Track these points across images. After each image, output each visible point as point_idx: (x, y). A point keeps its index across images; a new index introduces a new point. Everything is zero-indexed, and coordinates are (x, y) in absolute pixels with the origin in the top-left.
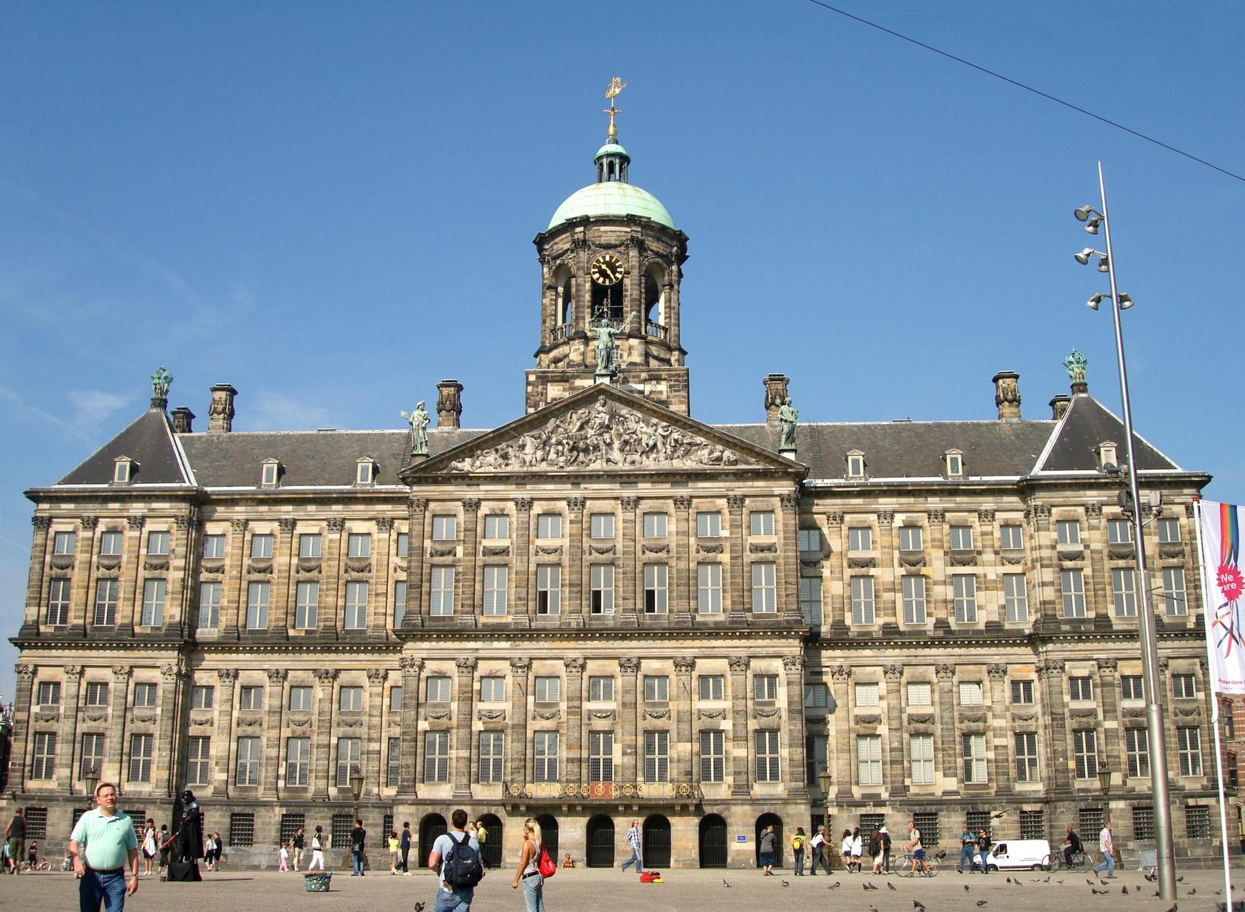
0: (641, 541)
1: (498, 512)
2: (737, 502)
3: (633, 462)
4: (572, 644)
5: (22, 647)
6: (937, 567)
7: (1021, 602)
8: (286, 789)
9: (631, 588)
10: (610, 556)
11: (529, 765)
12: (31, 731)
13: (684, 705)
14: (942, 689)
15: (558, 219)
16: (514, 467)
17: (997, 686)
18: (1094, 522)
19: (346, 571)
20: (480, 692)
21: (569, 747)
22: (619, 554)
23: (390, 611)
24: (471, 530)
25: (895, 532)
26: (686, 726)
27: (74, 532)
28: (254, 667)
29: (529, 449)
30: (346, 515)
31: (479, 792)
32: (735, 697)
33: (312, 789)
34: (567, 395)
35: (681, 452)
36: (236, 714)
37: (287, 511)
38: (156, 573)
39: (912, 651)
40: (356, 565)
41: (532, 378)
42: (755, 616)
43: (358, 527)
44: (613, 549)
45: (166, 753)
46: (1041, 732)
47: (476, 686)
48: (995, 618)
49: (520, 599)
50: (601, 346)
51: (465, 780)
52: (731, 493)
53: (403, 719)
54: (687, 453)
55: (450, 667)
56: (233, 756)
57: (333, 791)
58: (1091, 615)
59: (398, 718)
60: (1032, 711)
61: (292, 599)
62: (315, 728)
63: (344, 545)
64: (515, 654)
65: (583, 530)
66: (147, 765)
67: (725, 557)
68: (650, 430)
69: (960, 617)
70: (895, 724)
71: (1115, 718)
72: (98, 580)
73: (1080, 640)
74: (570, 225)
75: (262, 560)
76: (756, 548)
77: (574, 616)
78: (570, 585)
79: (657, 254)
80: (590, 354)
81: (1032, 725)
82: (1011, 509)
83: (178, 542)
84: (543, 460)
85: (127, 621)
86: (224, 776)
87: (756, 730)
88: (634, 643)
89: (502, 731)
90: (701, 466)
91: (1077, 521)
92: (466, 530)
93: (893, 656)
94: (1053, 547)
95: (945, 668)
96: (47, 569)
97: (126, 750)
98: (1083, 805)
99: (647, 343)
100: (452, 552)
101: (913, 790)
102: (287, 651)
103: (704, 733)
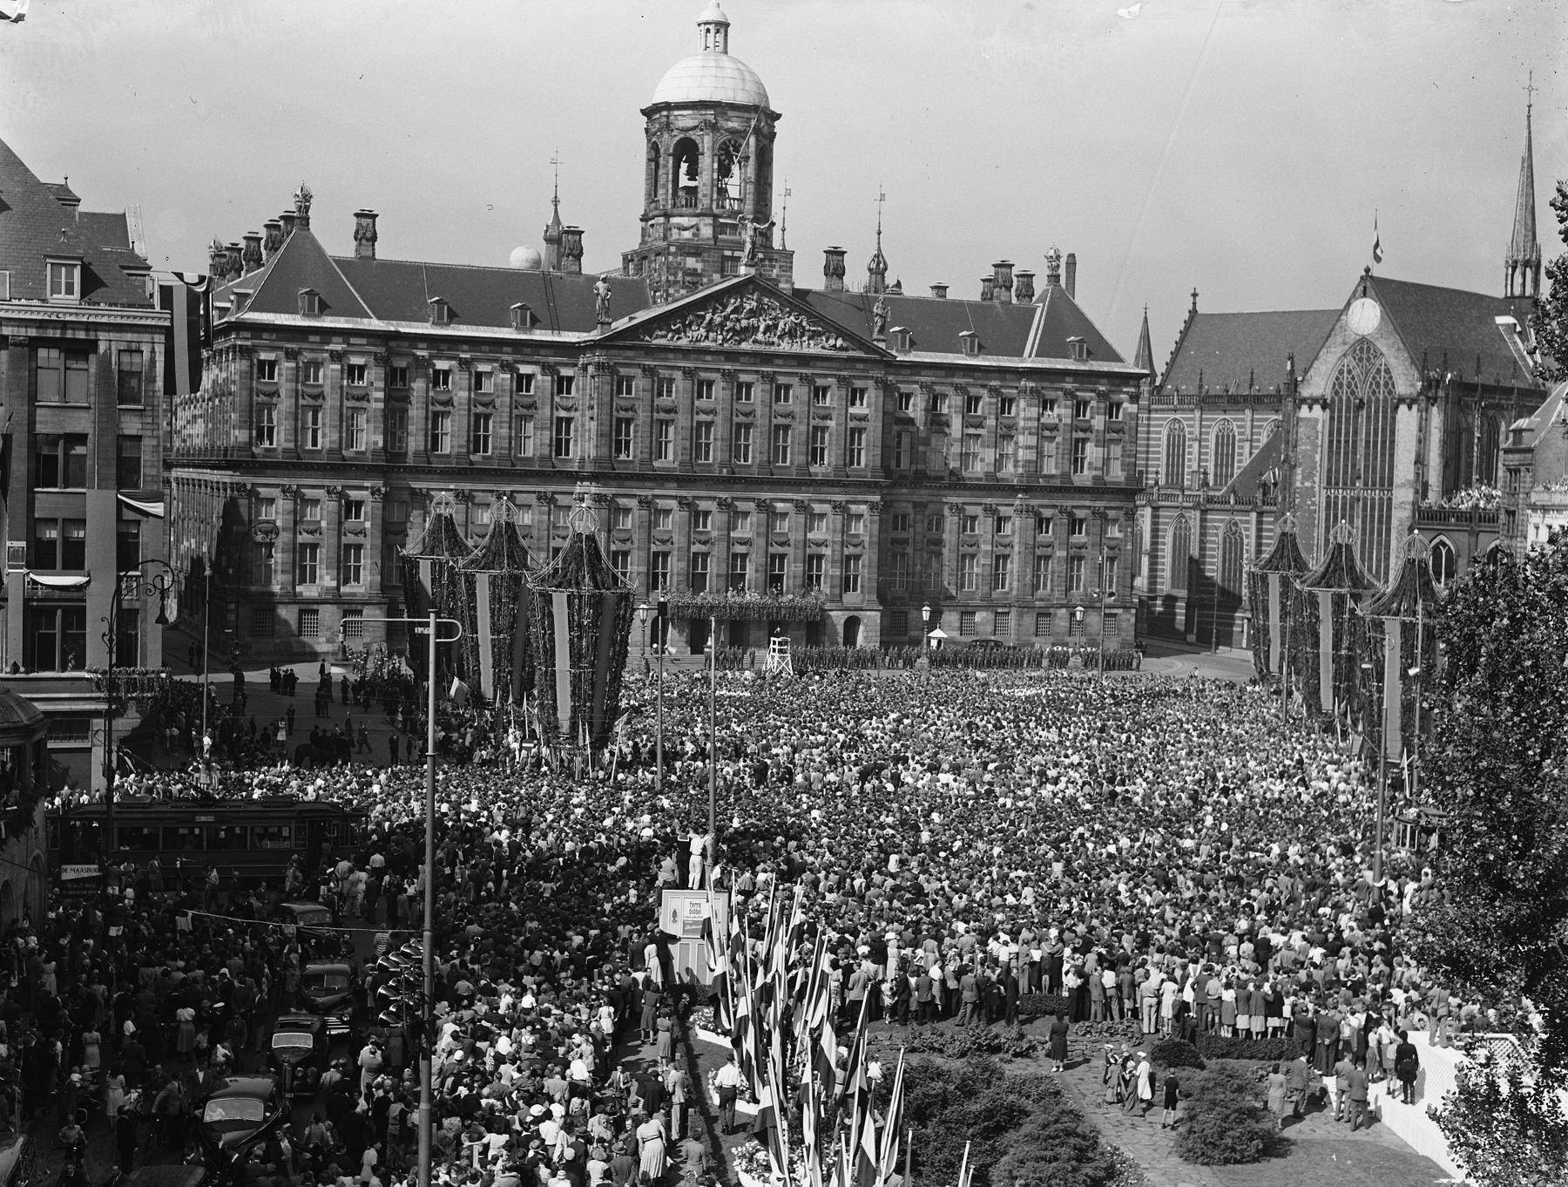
21: (718, 564)
26: (800, 552)
32: (834, 531)
34: (699, 266)
38: (358, 404)
43: (525, 369)
46: (1016, 558)
48: (992, 469)
58: (1058, 472)
60: (1007, 541)
64: (683, 493)
66: (357, 569)
67: (832, 424)
81: (1007, 551)
83: (374, 379)
85: (335, 446)
100: (632, 408)
103: (811, 557)
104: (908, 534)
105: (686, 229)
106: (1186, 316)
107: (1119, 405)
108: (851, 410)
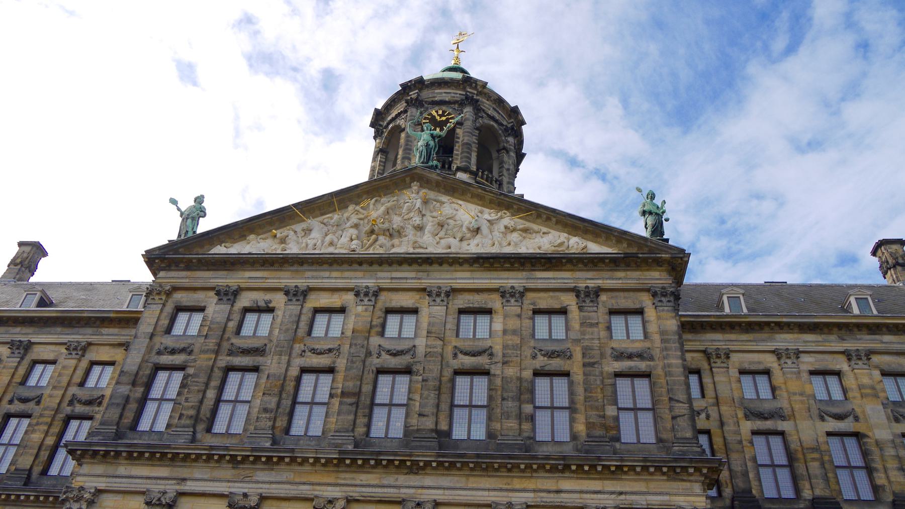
1: (262, 304)
4: (331, 480)
9: (432, 401)
19: (71, 403)
25: (805, 376)
29: (316, 235)
30: (94, 339)
49: (266, 410)
52: (582, 285)
63: (80, 373)
74: (406, 87)
76: (620, 356)
78: (343, 394)
79: (492, 118)
84: (331, 244)
88: (428, 481)
92: (212, 323)
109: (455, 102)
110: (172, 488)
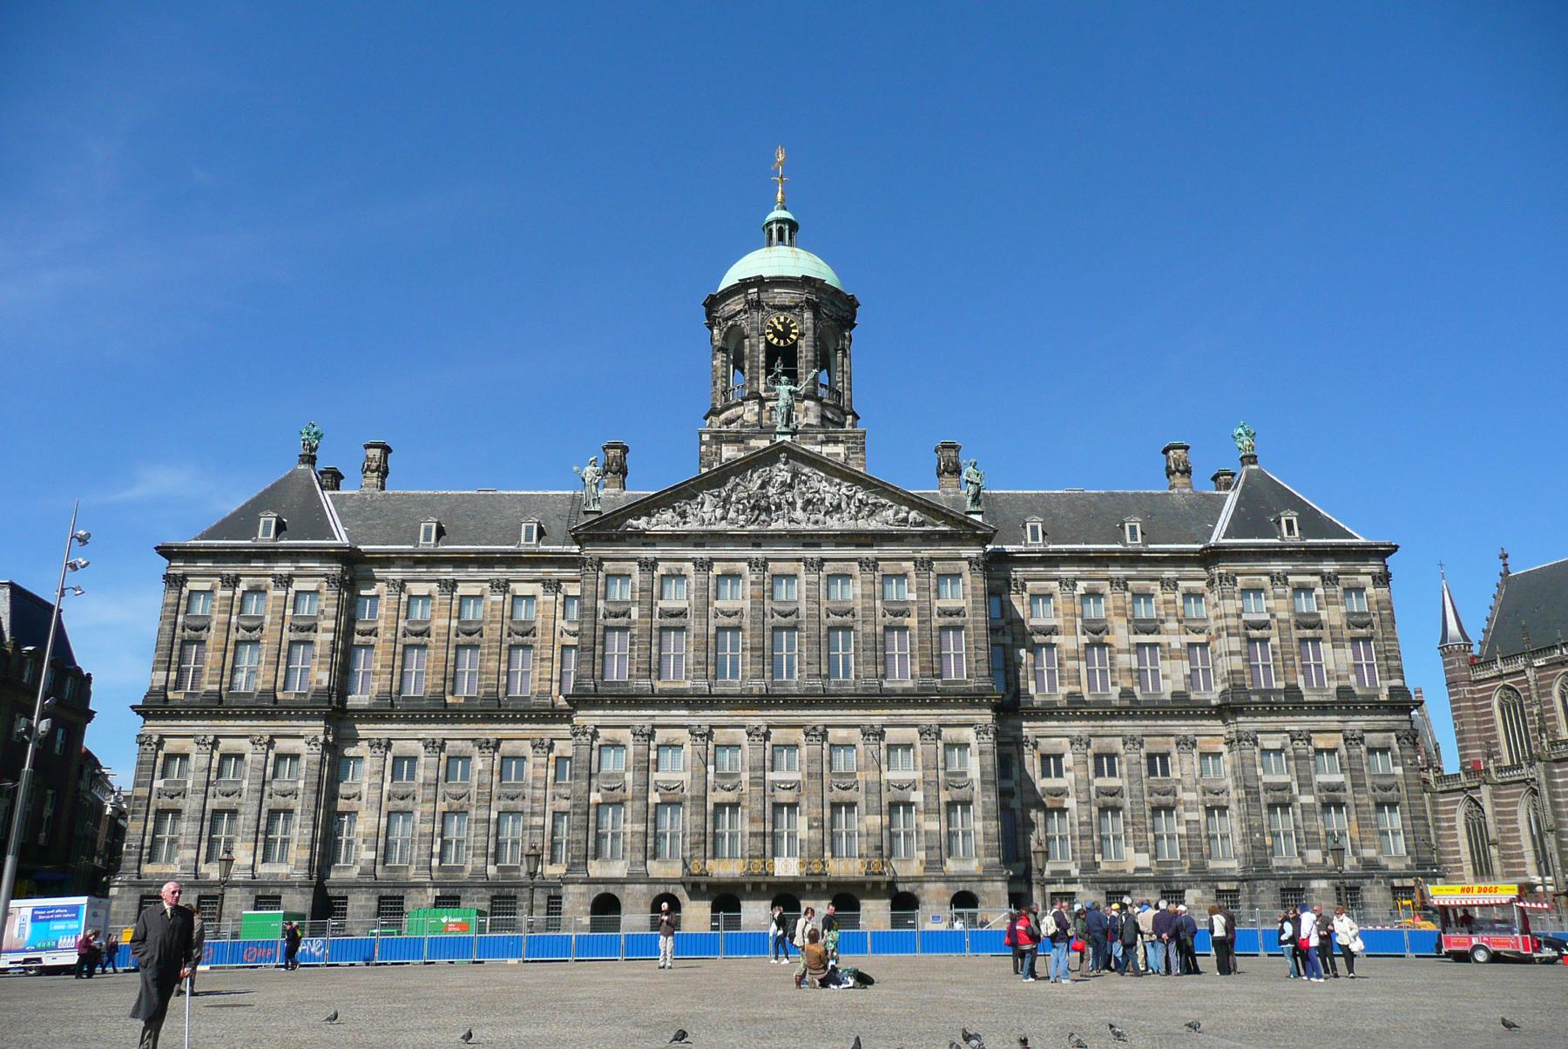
0: (825, 604)
2: (924, 565)
3: (816, 522)
5: (146, 716)
6: (1121, 635)
7: (1206, 671)
8: (440, 868)
10: (793, 618)
11: (709, 840)
12: (152, 808)
13: (872, 776)
14: (1129, 761)
15: (730, 279)
16: (693, 525)
17: (1186, 758)
18: (1280, 591)
20: (657, 762)
21: (752, 820)
22: (803, 617)
23: (556, 677)
24: (647, 591)
25: (1077, 599)
26: (876, 798)
27: (211, 591)
28: (409, 738)
31: (656, 869)
32: (925, 767)
33: (469, 867)
35: (865, 511)
36: (387, 786)
37: (447, 573)
38: (302, 636)
39: (1099, 723)
40: (521, 628)
41: (706, 437)
42: (944, 683)
43: (521, 589)
44: (796, 612)
45: (308, 831)
47: (653, 755)
48: (1181, 688)
50: (781, 403)
51: (640, 857)
53: (573, 791)
54: (872, 513)
55: (625, 736)
56: (382, 832)
57: (492, 870)
58: (1281, 685)
59: (564, 791)
61: (450, 664)
62: (473, 802)
64: (694, 721)
65: (765, 593)
66: (285, 842)
68: (834, 490)
69: (1143, 687)
70: (1083, 797)
71: (1312, 793)
72: (237, 643)
73: (1271, 712)
74: (744, 285)
75: (419, 622)
76: (944, 613)
77: (757, 681)
80: (765, 415)
82: (1194, 578)
84: (723, 518)
85: (269, 686)
86: (372, 855)
87: (948, 804)
89: (680, 804)
90: (886, 527)
91: (1262, 590)
93: (1078, 728)
94: (1239, 616)
95: (1133, 739)
96: (179, 631)
97: (262, 828)
98: (1283, 884)
99: (824, 406)
100: (626, 614)
101: (1104, 866)
102: (444, 721)
103: (893, 806)
104: (1067, 780)
105: (733, 421)
106: (1499, 579)
107: (1360, 590)
108: (938, 604)
109: (796, 306)
110: (648, 723)
